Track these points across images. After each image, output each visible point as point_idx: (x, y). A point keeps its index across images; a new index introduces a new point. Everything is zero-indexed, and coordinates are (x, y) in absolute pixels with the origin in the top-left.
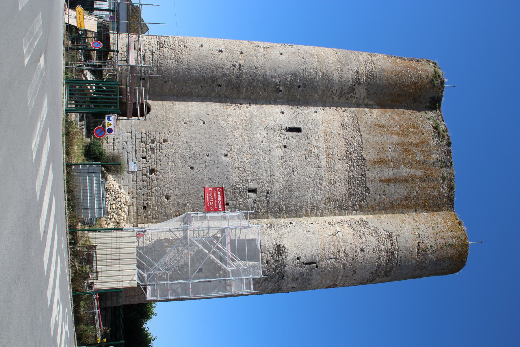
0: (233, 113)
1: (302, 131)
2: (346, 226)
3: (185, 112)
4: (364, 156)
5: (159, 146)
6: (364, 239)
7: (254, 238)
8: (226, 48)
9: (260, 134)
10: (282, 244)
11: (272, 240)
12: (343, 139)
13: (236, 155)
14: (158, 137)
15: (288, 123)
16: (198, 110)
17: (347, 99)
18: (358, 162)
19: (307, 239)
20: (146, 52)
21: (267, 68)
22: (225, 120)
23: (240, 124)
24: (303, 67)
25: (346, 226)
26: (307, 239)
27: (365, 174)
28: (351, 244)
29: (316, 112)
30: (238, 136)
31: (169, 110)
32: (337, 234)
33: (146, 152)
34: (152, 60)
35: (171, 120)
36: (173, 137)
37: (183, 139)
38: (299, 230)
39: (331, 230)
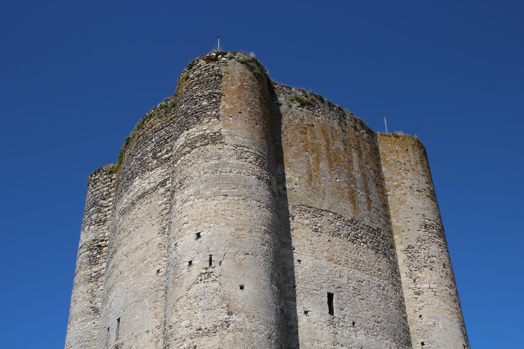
1: (332, 292)
2: (419, 275)
4: (350, 218)
6: (434, 259)
12: (335, 238)
18: (358, 229)
21: (269, 319)
24: (260, 258)
25: (419, 275)
27: (367, 226)
28: (442, 277)
32: (434, 290)
39: (427, 295)
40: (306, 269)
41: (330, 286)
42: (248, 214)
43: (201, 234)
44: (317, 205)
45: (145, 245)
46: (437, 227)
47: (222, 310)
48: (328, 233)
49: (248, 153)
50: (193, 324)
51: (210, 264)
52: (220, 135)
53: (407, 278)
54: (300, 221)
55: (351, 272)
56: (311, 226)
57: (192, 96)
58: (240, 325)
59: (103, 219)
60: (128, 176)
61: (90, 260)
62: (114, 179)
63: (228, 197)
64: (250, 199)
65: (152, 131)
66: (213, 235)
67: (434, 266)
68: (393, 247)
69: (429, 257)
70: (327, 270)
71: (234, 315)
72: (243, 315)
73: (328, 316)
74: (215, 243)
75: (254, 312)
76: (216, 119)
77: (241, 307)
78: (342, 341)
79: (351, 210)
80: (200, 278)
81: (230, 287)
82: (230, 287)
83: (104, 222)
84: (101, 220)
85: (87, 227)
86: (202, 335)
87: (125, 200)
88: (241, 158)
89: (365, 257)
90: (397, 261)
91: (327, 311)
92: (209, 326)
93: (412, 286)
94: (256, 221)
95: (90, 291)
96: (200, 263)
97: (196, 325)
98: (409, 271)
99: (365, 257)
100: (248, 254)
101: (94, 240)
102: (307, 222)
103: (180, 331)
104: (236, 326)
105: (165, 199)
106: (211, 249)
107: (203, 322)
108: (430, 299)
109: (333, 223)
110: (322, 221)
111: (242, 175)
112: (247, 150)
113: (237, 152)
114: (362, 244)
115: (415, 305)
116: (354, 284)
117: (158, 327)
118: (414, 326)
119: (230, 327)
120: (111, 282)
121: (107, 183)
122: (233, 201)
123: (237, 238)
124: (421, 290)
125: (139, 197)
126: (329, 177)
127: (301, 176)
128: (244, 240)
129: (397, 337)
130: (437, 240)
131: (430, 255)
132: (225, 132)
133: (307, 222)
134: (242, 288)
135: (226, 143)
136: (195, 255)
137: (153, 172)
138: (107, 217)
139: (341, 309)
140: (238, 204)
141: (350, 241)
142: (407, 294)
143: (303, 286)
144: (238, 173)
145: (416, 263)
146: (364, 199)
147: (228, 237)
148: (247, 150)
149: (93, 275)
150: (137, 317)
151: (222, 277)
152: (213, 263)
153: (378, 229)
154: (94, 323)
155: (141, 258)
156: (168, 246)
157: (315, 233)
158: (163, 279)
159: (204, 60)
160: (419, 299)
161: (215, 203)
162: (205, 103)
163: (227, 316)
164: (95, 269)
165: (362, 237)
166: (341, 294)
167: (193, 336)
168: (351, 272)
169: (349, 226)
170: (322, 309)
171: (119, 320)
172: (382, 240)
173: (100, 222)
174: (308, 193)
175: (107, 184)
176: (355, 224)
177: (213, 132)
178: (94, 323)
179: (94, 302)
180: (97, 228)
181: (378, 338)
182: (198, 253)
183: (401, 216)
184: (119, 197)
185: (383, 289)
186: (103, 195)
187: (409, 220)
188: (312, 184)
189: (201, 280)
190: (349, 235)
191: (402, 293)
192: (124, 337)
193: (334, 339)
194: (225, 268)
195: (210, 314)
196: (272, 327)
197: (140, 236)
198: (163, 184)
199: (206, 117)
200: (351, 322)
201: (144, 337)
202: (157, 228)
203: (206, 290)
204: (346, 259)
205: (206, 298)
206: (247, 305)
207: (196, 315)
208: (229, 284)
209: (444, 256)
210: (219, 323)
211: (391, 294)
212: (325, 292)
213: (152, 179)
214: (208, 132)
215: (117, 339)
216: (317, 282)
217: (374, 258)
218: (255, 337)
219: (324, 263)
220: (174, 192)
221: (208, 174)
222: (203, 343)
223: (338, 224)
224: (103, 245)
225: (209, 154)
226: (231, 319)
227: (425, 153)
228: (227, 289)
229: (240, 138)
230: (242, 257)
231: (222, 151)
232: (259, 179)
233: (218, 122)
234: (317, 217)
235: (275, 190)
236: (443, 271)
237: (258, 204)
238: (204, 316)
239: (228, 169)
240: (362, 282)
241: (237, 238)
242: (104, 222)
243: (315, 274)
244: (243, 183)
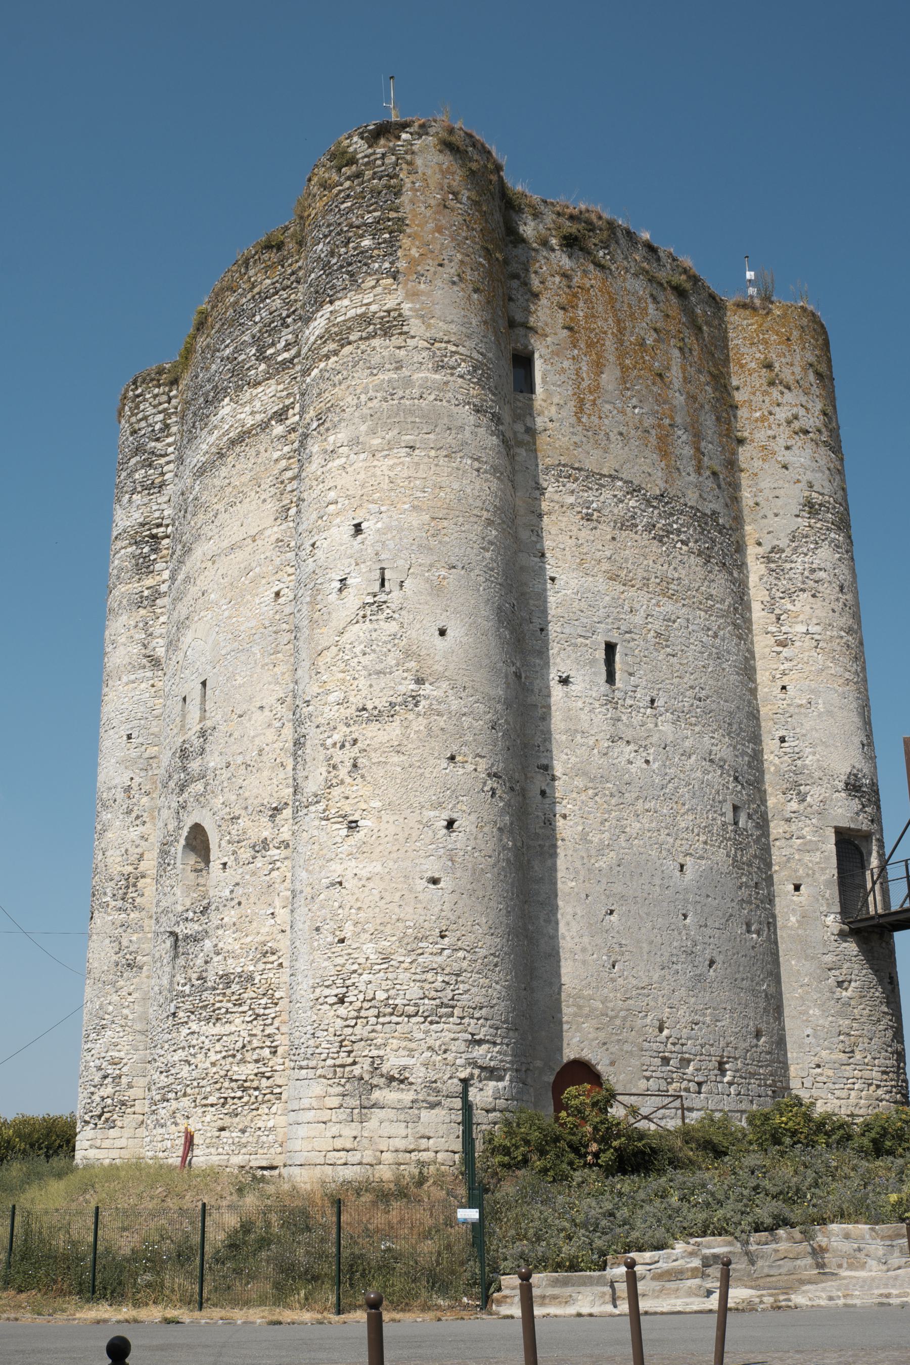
0: (577, 824)
1: (614, 641)
2: (789, 606)
3: (584, 962)
4: (658, 492)
5: (674, 1044)
6: (822, 574)
7: (832, 839)
8: (440, 805)
9: (631, 763)
10: (843, 778)
11: (838, 800)
12: (625, 534)
13: (679, 842)
14: (654, 1046)
16: (573, 923)
18: (672, 515)
19: (830, 713)
20: (474, 1064)
21: (493, 693)
22: (600, 852)
23: (610, 812)
24: (477, 575)
25: (789, 606)
26: (830, 713)
27: (691, 507)
28: (834, 611)
30: (639, 825)
31: (580, 1007)
32: (817, 637)
33: (689, 1081)
34: (495, 1044)
35: (610, 1005)
36: (652, 1004)
37: (656, 978)
38: (807, 726)
40: (566, 595)
41: (610, 630)
42: (456, 486)
43: (363, 526)
44: (590, 464)
45: (249, 540)
46: (835, 508)
47: (405, 674)
48: (612, 524)
49: (457, 357)
50: (351, 699)
51: (383, 585)
52: (400, 315)
53: (763, 613)
54: (556, 497)
55: (654, 601)
56: (579, 509)
57: (340, 224)
58: (440, 703)
59: (157, 481)
60: (206, 394)
61: (137, 565)
62: (175, 397)
63: (417, 451)
64: (459, 455)
65: (253, 297)
66: (389, 528)
67: (821, 589)
68: (740, 548)
69: (813, 571)
70: (607, 598)
71: (427, 685)
72: (445, 685)
73: (604, 688)
74: (391, 544)
75: (466, 679)
76: (390, 281)
77: (441, 669)
78: (629, 734)
79: (660, 474)
80: (361, 613)
81: (421, 631)
82: (421, 631)
83: (160, 487)
84: (153, 483)
85: (127, 496)
86: (369, 720)
87: (204, 447)
88: (443, 367)
89: (684, 572)
90: (748, 577)
91: (604, 676)
92: (381, 703)
94: (471, 501)
95: (141, 625)
96: (361, 584)
97: (356, 700)
98: (768, 599)
99: (683, 572)
100: (454, 567)
101: (143, 525)
102: (571, 500)
103: (326, 710)
104: (431, 704)
105: (286, 449)
106: (383, 557)
107: (369, 697)
108: (807, 654)
109: (622, 501)
110: (602, 499)
111: (444, 403)
112: (454, 349)
113: (434, 353)
114: (679, 545)
115: (775, 666)
116: (658, 625)
117: (282, 701)
118: (769, 707)
119: (420, 707)
120: (182, 610)
121: (160, 404)
122: (426, 460)
123: (433, 536)
124: (790, 636)
125: (233, 443)
126: (619, 404)
127: (562, 402)
128: (447, 539)
129: (735, 727)
130: (832, 535)
131: (814, 566)
132: (410, 309)
133: (571, 500)
134: (442, 633)
135: (412, 333)
136: (352, 567)
137: (260, 389)
138: (166, 477)
139: (631, 674)
140: (436, 465)
141: (654, 538)
142: (762, 644)
143: (559, 630)
144: (436, 400)
145: (785, 582)
146: (688, 451)
147: (417, 533)
148: (454, 349)
149: (146, 593)
150: (240, 681)
151: (403, 612)
152: (386, 583)
153: (714, 513)
154: (153, 686)
155: (242, 566)
156: (296, 547)
157: (586, 523)
158: (288, 610)
159: (362, 138)
160: (784, 654)
161: (391, 462)
162: (366, 242)
163: (413, 686)
164: (149, 581)
165: (679, 532)
166: (632, 644)
167: (352, 722)
168: (654, 601)
169: (655, 507)
170: (595, 674)
171: (204, 684)
172: (720, 536)
173: (155, 487)
174: (576, 439)
175: (161, 408)
176: (667, 503)
177: (385, 308)
178: (153, 686)
179: (150, 647)
180: (146, 500)
181: (697, 729)
182: (357, 564)
183: (762, 485)
184: (189, 438)
185: (715, 636)
186: (153, 431)
187: (777, 492)
188: (584, 420)
189: (364, 617)
190: (654, 526)
191: (752, 643)
192: (215, 717)
193: (612, 729)
194: (409, 593)
195: (383, 681)
196: (499, 707)
197: (239, 523)
198: (281, 416)
199: (369, 274)
200: (649, 698)
201: (254, 718)
202: (272, 507)
203: (374, 635)
204: (645, 574)
205: (374, 651)
206: (452, 666)
207: (356, 682)
208: (418, 626)
209: (843, 571)
210: (400, 699)
211: (731, 644)
212: (601, 639)
213: (257, 404)
214: (374, 308)
215: (202, 719)
216: (585, 621)
217: (701, 572)
218: (466, 725)
219: (601, 585)
220: (305, 436)
221: (375, 401)
222: (370, 735)
223: (632, 503)
224: (160, 535)
225: (376, 360)
226: (421, 692)
227: (826, 343)
228: (414, 635)
229: (441, 324)
230: (443, 573)
231: (403, 352)
232: (478, 411)
233: (395, 287)
234: (591, 489)
235: (509, 435)
236: (837, 600)
237: (476, 465)
238: (371, 686)
239: (416, 392)
240: (674, 622)
241: (433, 536)
242: (160, 487)
243: (583, 605)
244: (446, 421)
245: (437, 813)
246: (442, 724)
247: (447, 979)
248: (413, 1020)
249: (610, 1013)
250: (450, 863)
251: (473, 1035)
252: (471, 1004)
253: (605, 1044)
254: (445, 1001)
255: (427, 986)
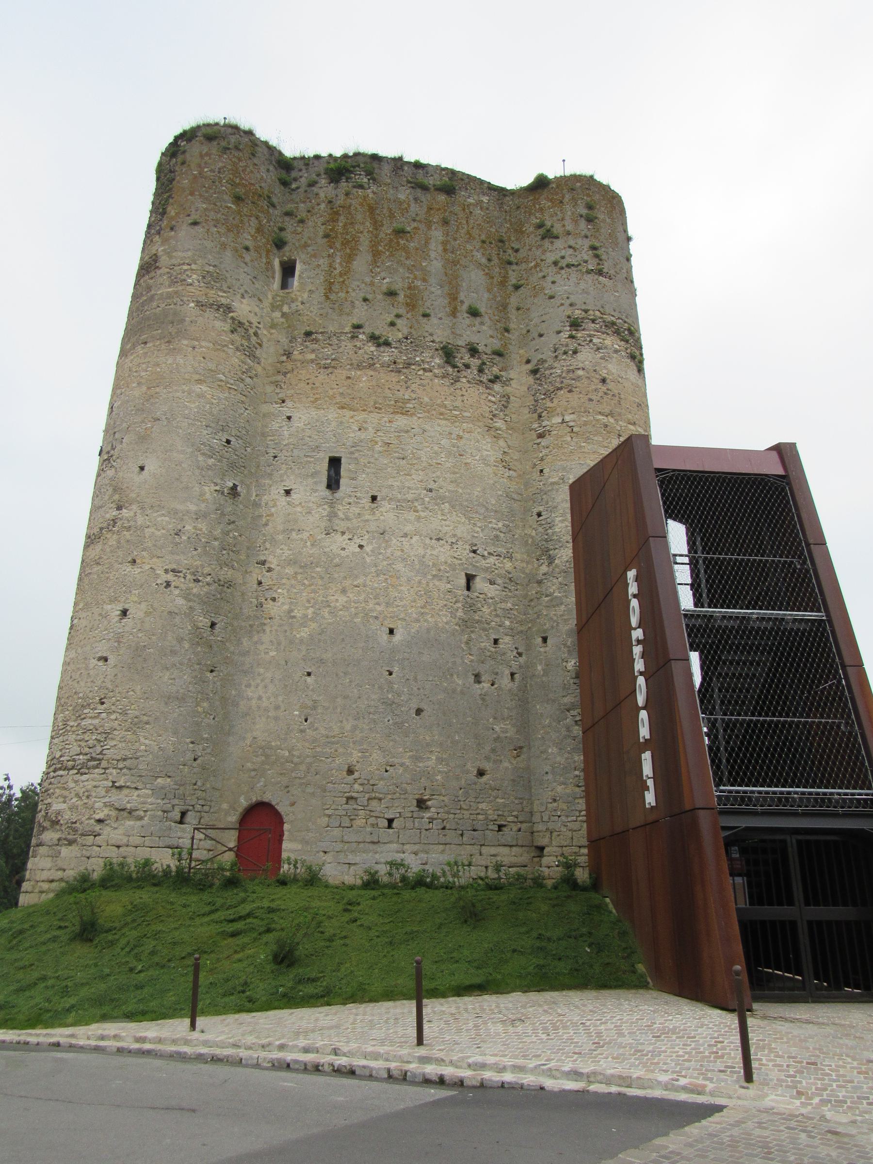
2: (549, 404)
3: (276, 719)
8: (114, 600)
15: (316, 483)
17: (260, 345)
25: (549, 404)
29: (289, 418)
32: (571, 424)
93: (535, 425)
98: (533, 403)
160: (543, 444)
170: (316, 483)
187: (544, 318)
210: (105, 525)
245: (113, 606)
246: (128, 537)
247: (99, 737)
248: (72, 772)
249: (296, 760)
250: (116, 644)
251: (114, 782)
252: (115, 757)
253: (287, 787)
254: (94, 755)
255: (83, 744)
